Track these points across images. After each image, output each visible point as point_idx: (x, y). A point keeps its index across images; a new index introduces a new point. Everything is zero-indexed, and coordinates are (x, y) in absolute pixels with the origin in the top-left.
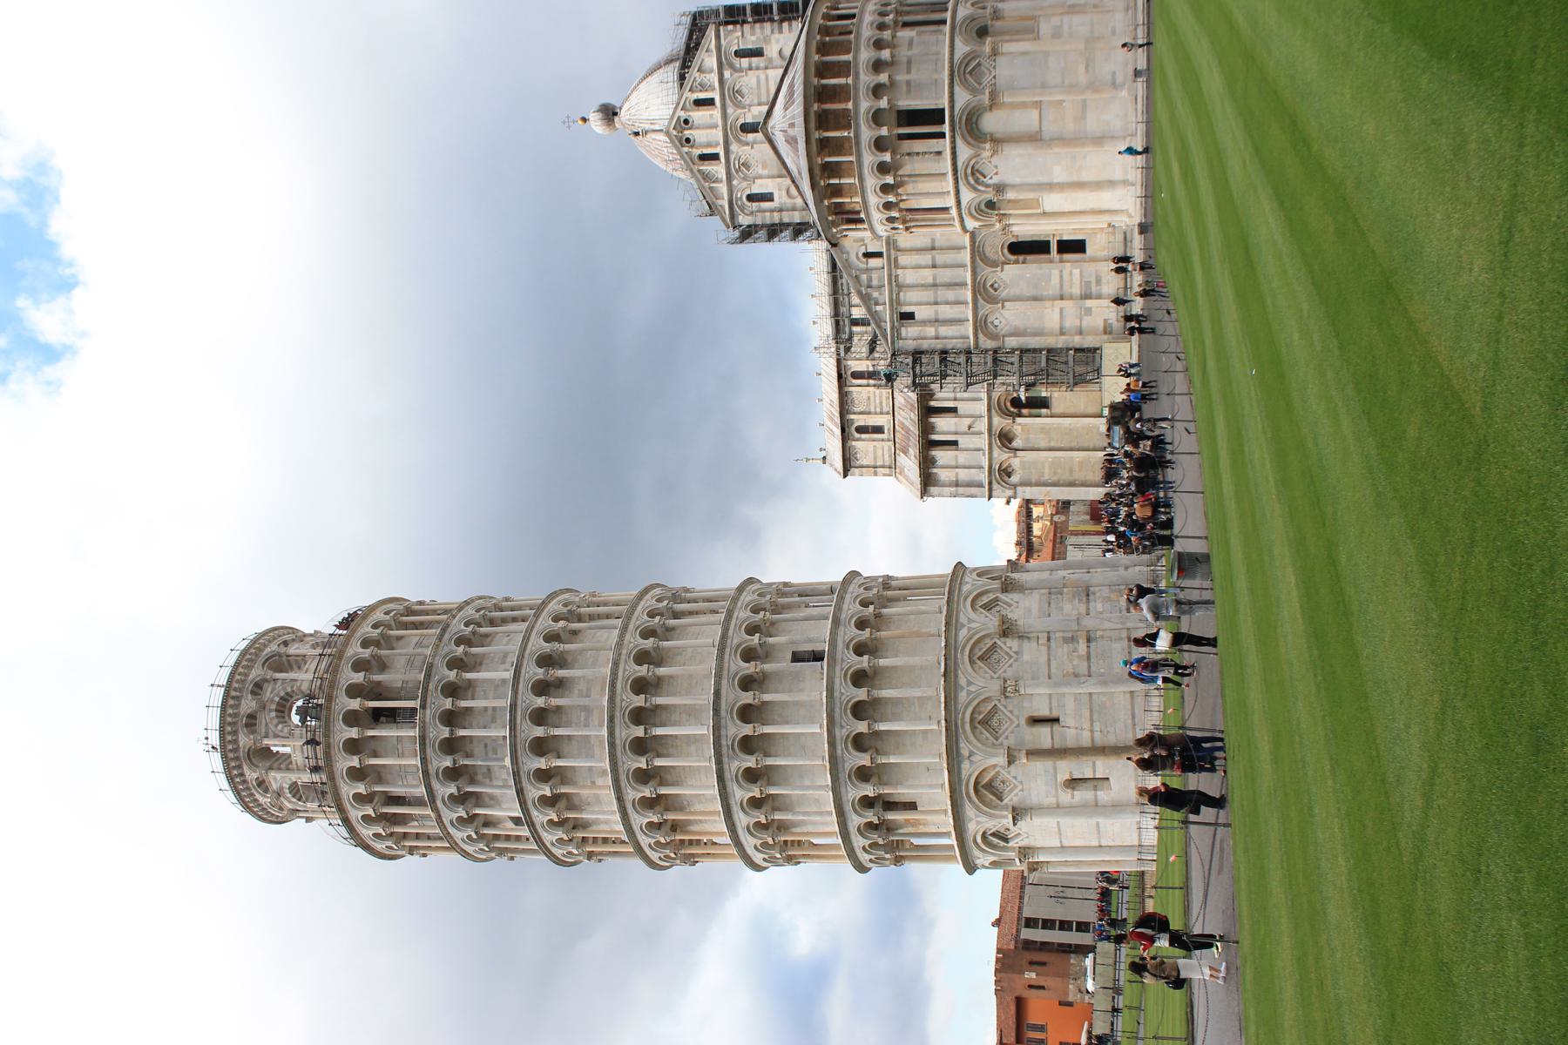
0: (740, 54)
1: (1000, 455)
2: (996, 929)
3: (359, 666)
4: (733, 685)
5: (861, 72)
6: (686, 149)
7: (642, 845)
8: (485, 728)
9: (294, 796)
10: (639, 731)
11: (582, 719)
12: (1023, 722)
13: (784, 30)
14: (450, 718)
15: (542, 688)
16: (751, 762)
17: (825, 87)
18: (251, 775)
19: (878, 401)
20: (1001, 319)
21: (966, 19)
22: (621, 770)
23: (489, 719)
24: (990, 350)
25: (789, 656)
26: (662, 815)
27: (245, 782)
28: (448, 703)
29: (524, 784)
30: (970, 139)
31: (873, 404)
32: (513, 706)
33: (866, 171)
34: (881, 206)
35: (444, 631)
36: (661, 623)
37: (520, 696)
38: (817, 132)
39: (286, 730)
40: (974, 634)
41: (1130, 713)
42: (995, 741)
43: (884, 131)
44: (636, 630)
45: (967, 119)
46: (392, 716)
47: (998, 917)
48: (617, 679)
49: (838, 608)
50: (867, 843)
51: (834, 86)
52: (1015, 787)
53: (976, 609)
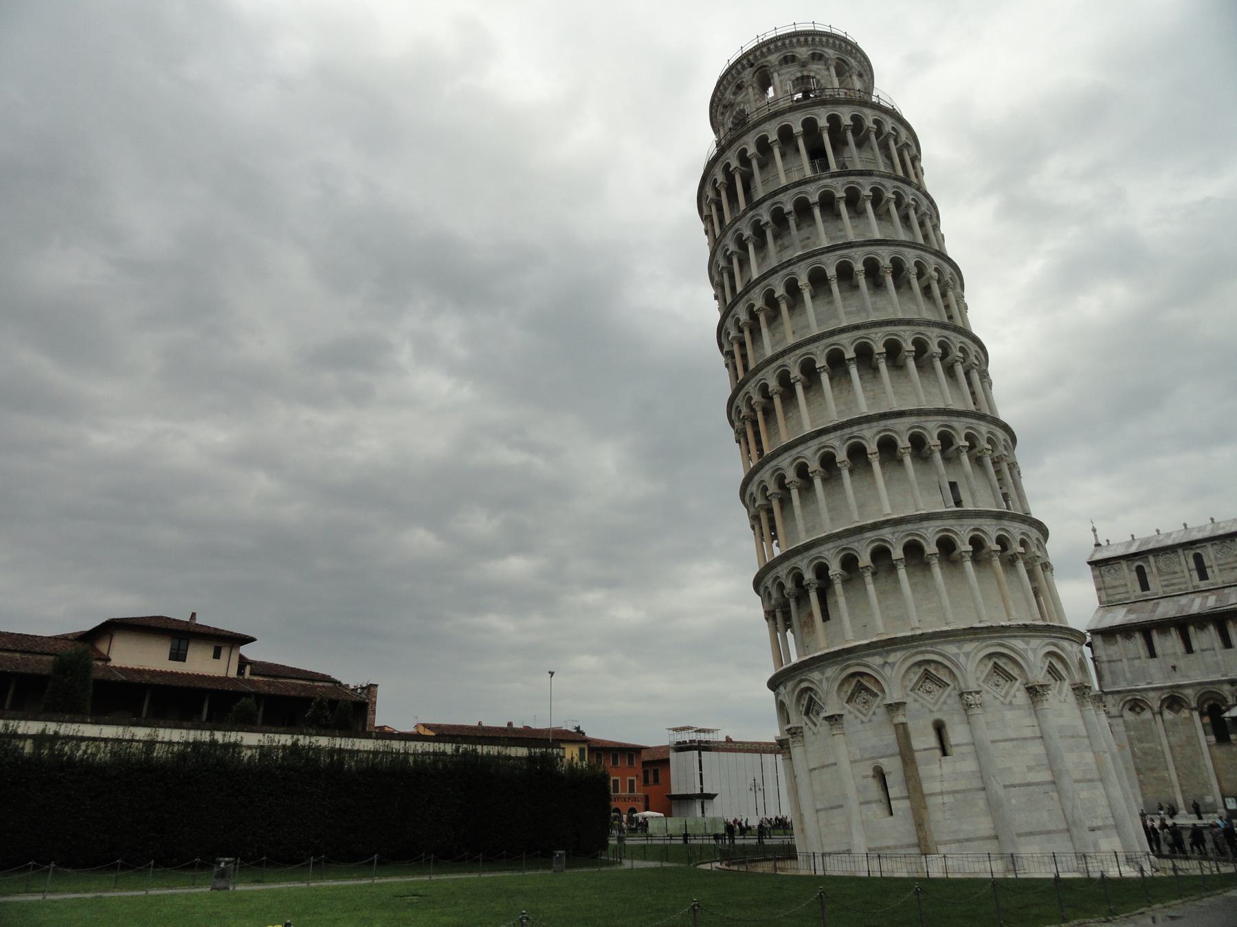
2: (725, 740)
7: (746, 387)
11: (850, 309)
12: (937, 716)
14: (828, 202)
15: (872, 268)
16: (841, 456)
18: (747, 75)
19: (1174, 581)
22: (809, 347)
23: (833, 235)
27: (739, 73)
29: (781, 273)
31: (1170, 577)
32: (850, 245)
36: (957, 358)
41: (971, 836)
47: (733, 740)
52: (865, 715)
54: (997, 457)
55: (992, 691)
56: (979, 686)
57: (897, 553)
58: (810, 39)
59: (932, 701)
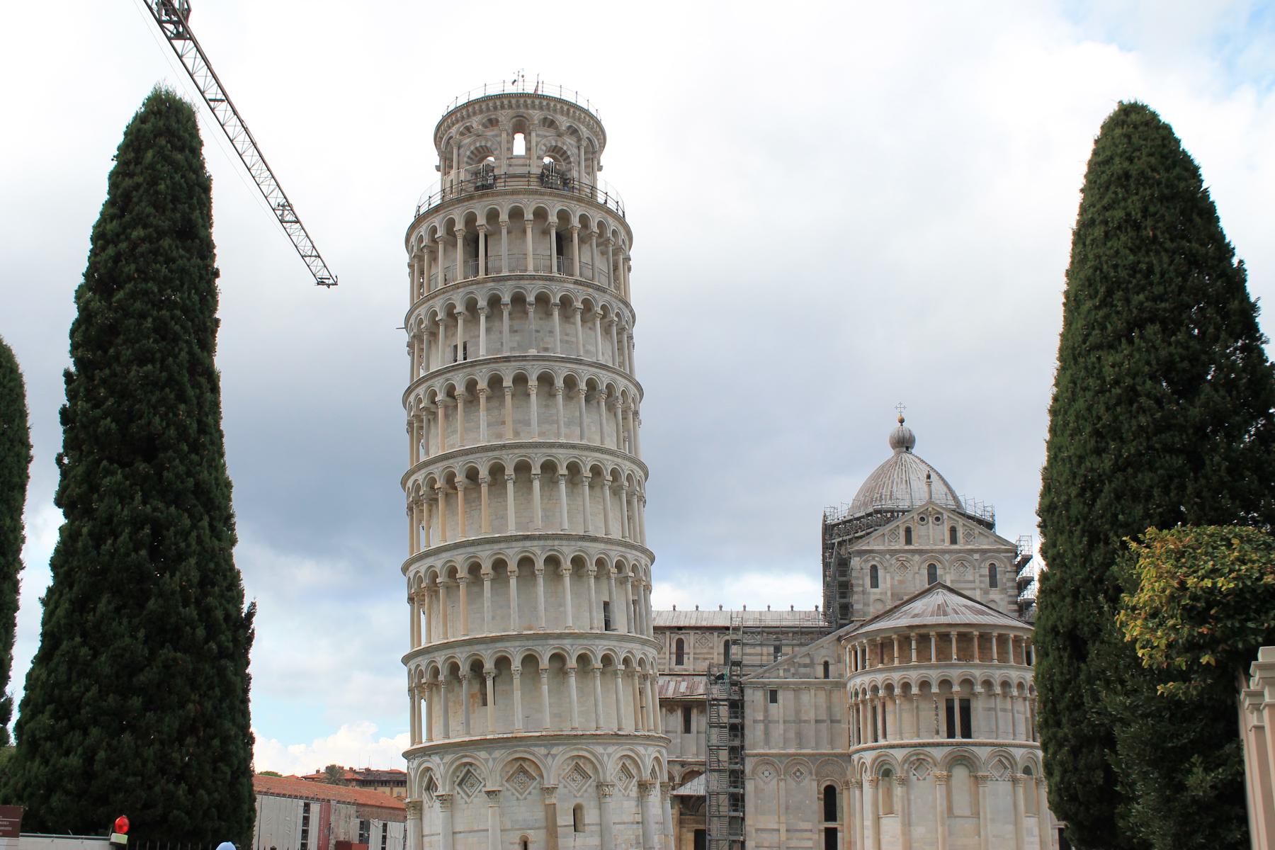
0: (993, 568)
4: (600, 553)
5: (1002, 671)
7: (451, 461)
10: (563, 470)
12: (579, 801)
21: (1037, 757)
24: (744, 767)
27: (495, 108)
30: (950, 758)
32: (579, 362)
37: (586, 368)
39: (541, 153)
43: (956, 688)
51: (991, 649)
52: (521, 794)
57: (572, 663)
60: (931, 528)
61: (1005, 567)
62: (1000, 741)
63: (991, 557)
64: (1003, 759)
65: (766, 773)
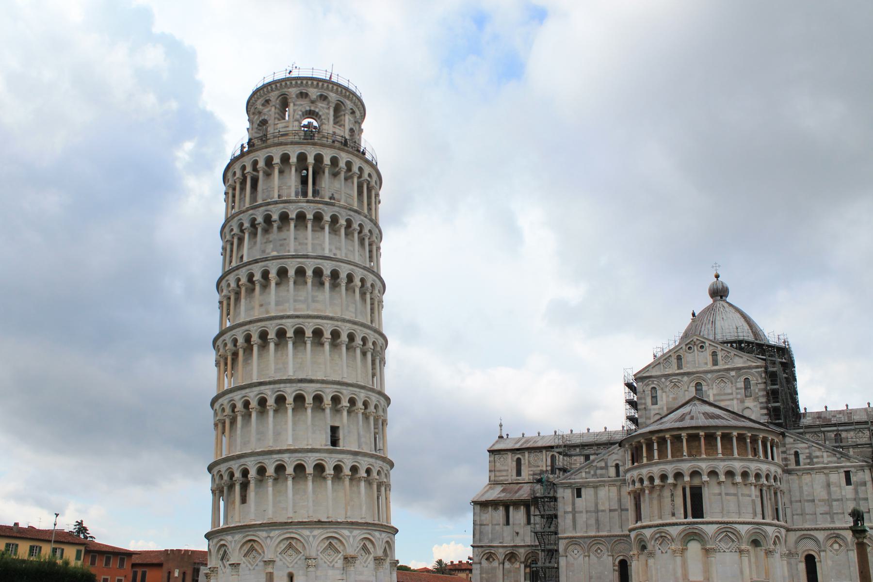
1: (500, 553)
3: (334, 161)
5: (726, 463)
6: (684, 347)
7: (225, 336)
8: (295, 238)
9: (260, 122)
10: (290, 334)
12: (290, 570)
13: (763, 410)
14: (301, 217)
15: (318, 273)
16: (271, 401)
17: (716, 439)
18: (274, 96)
20: (578, 555)
25: (336, 424)
26: (241, 348)
27: (268, 92)
28: (310, 216)
29: (260, 264)
30: (683, 535)
32: (307, 257)
33: (662, 467)
34: (641, 476)
35: (356, 211)
36: (358, 345)
37: (313, 260)
38: (686, 435)
39: (298, 117)
40: (345, 539)
42: (279, 553)
43: (687, 479)
44: (353, 330)
45: (695, 532)
46: (304, 181)
48: (322, 319)
49: (365, 455)
50: (223, 473)
51: (716, 445)
52: (252, 565)
53: (363, 541)
54: (369, 413)
55: (324, 559)
56: (318, 555)
58: (320, 84)
59: (290, 561)
60: (696, 355)
61: (757, 380)
62: (726, 519)
63: (746, 373)
64: (728, 533)
65: (576, 552)
